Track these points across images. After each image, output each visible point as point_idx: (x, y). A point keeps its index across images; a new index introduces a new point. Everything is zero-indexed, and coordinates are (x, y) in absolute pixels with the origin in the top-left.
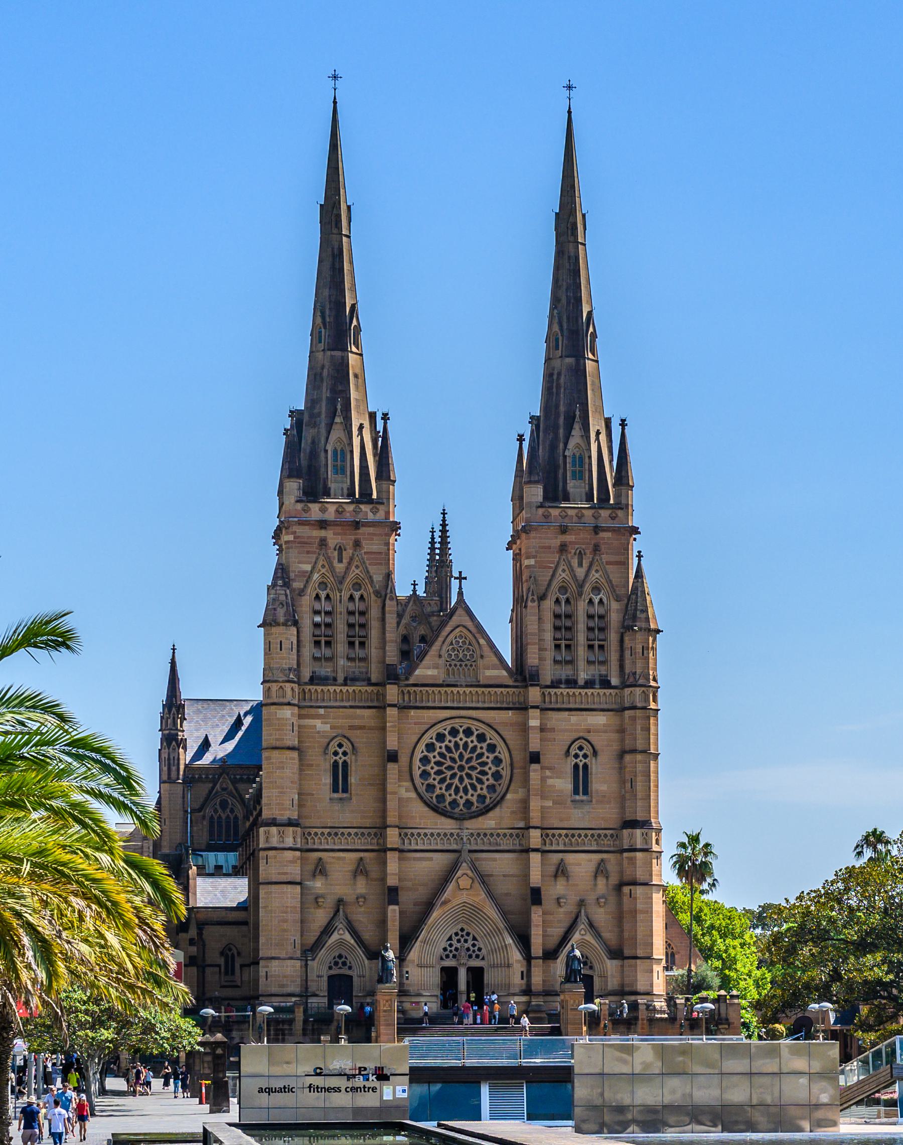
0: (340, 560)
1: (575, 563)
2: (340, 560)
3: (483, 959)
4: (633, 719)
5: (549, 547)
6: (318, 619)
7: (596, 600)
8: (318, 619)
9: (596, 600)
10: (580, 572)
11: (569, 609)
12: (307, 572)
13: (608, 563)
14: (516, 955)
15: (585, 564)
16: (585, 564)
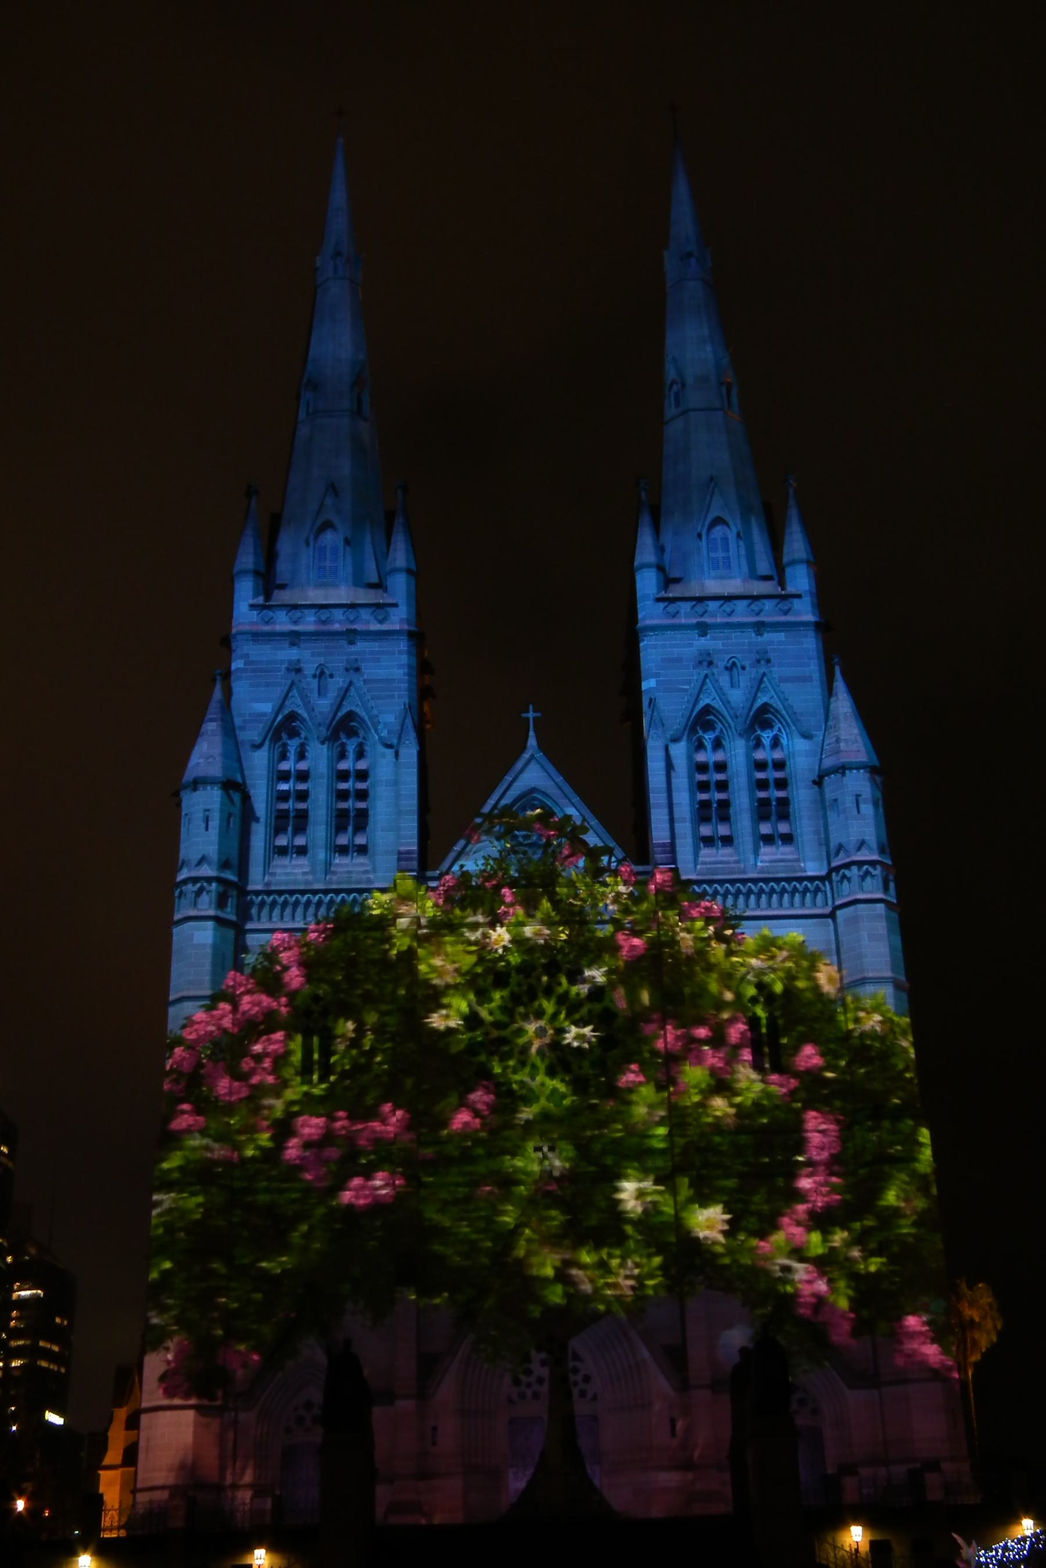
0: (321, 692)
1: (724, 680)
2: (321, 692)
3: (595, 1398)
4: (854, 920)
5: (679, 660)
6: (284, 787)
7: (766, 741)
8: (284, 787)
9: (766, 741)
10: (737, 696)
11: (719, 756)
12: (264, 714)
13: (783, 680)
14: (660, 1383)
15: (745, 680)
16: (745, 680)
